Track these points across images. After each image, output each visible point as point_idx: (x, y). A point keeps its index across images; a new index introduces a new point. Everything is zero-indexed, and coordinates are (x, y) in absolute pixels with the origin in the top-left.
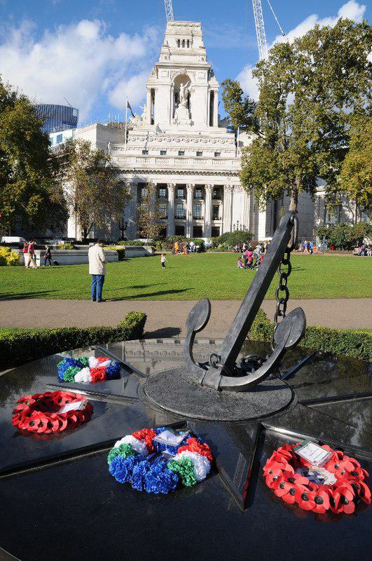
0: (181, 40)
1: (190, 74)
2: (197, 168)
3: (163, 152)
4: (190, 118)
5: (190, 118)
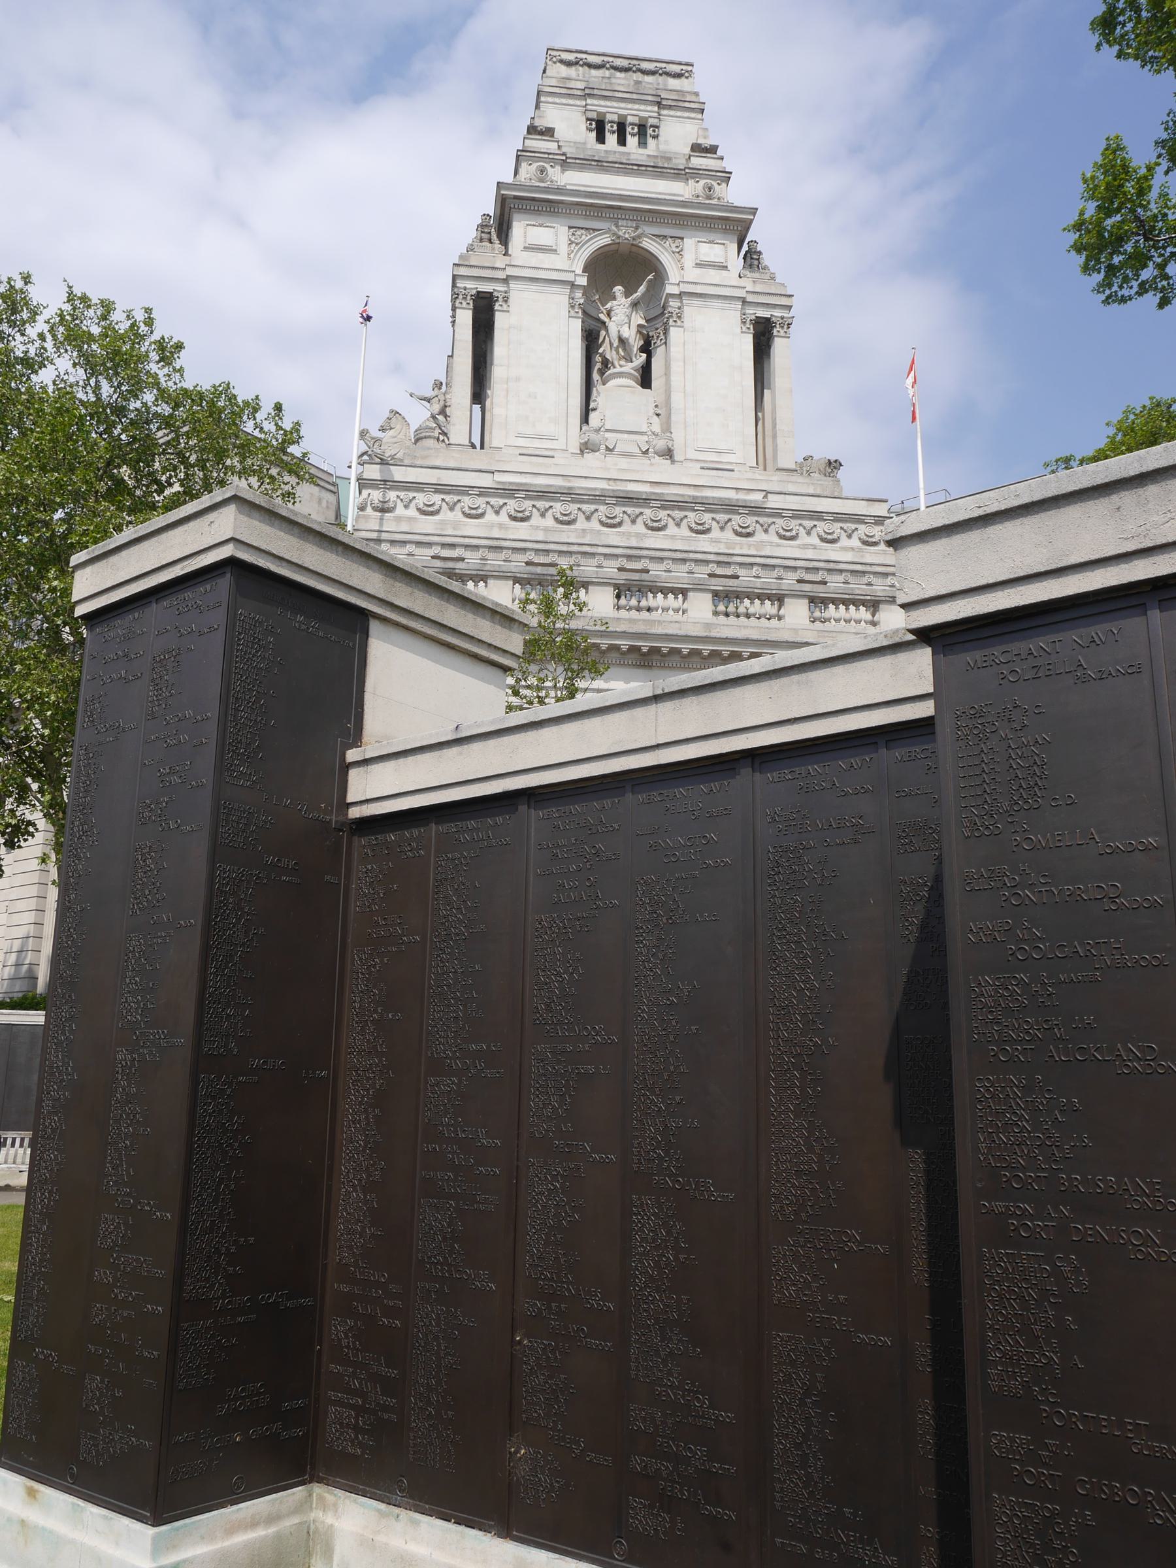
4: (667, 428)
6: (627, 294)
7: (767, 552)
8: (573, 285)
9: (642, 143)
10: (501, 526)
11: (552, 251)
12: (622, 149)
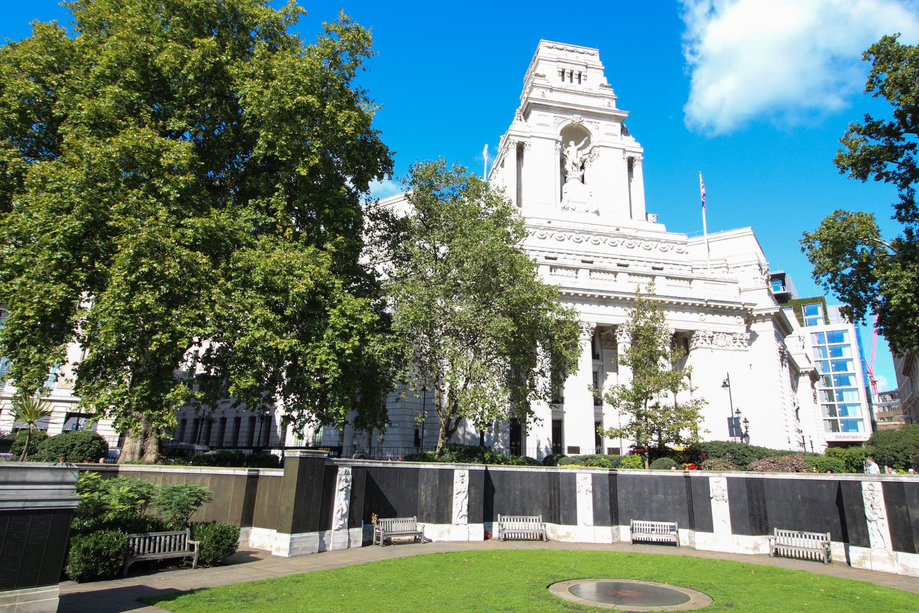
0: (568, 71)
1: (587, 123)
6: (576, 144)
8: (557, 141)
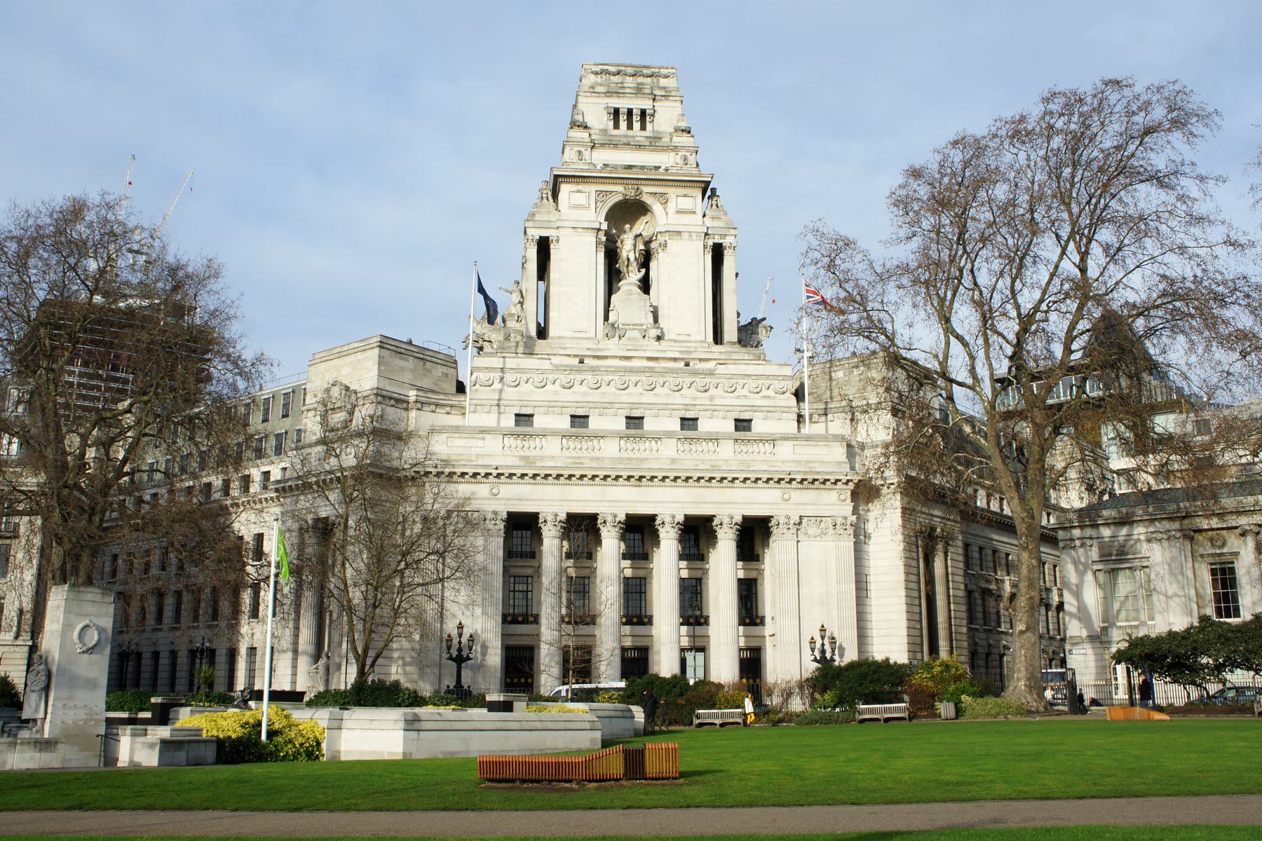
0: (623, 111)
1: (647, 194)
2: (688, 464)
3: (579, 420)
4: (656, 320)
5: (656, 320)
7: (717, 402)
8: (599, 230)
9: (643, 128)
10: (556, 393)
11: (582, 211)
12: (630, 133)
